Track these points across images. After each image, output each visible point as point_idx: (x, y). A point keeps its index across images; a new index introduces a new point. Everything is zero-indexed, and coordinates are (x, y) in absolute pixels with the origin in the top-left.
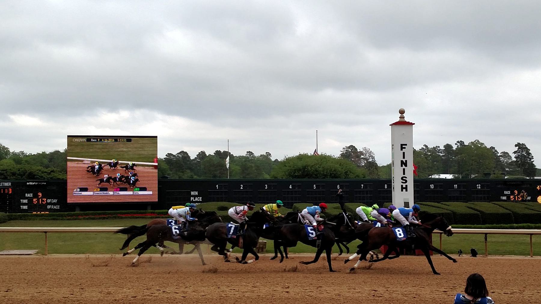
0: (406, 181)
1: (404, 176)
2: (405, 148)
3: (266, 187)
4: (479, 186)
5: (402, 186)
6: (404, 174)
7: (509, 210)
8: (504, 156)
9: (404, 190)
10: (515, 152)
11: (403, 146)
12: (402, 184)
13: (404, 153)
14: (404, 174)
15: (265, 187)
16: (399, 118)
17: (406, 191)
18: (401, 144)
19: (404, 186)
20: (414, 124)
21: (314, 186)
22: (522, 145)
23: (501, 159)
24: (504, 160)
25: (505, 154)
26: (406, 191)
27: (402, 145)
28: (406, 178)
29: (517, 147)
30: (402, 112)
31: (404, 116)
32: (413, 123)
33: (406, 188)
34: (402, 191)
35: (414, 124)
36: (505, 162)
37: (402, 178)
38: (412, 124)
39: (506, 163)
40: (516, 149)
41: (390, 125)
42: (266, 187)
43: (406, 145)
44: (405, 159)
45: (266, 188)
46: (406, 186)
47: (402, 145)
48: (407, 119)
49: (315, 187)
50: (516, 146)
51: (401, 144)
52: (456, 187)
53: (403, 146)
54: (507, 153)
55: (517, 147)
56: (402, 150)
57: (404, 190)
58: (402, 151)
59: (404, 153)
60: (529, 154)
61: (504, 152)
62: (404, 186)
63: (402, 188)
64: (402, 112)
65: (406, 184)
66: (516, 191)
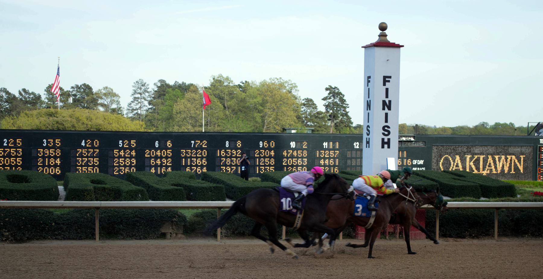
0: (389, 133)
1: (386, 124)
2: (389, 81)
3: (45, 142)
4: (356, 145)
5: (383, 139)
6: (386, 121)
7: (436, 181)
8: (307, 104)
9: (386, 146)
10: (324, 99)
11: (387, 79)
12: (384, 137)
13: (387, 90)
14: (386, 121)
15: (43, 143)
16: (378, 37)
17: (389, 147)
18: (384, 76)
19: (386, 140)
20: (403, 46)
21: (120, 143)
22: (334, 88)
23: (303, 108)
24: (307, 111)
25: (309, 103)
26: (389, 147)
27: (385, 77)
28: (388, 127)
29: (328, 92)
30: (383, 27)
31: (387, 33)
32: (401, 45)
33: (388, 143)
34: (383, 147)
35: (403, 46)
36: (308, 113)
37: (384, 128)
38: (399, 46)
39: (310, 114)
40: (326, 94)
41: (362, 47)
42: (45, 142)
43: (390, 77)
44: (389, 99)
45: (44, 145)
46: (389, 139)
47: (385, 77)
48: (391, 38)
49: (120, 145)
50: (327, 89)
51: (384, 76)
52: (326, 146)
53: (387, 79)
54: (311, 100)
55: (328, 92)
56: (384, 85)
57: (386, 146)
58: (385, 87)
59: (387, 90)
60: (343, 101)
61: (308, 99)
62: (386, 140)
63: (383, 143)
64: (383, 27)
65: (388, 137)
66: (133, 160)
